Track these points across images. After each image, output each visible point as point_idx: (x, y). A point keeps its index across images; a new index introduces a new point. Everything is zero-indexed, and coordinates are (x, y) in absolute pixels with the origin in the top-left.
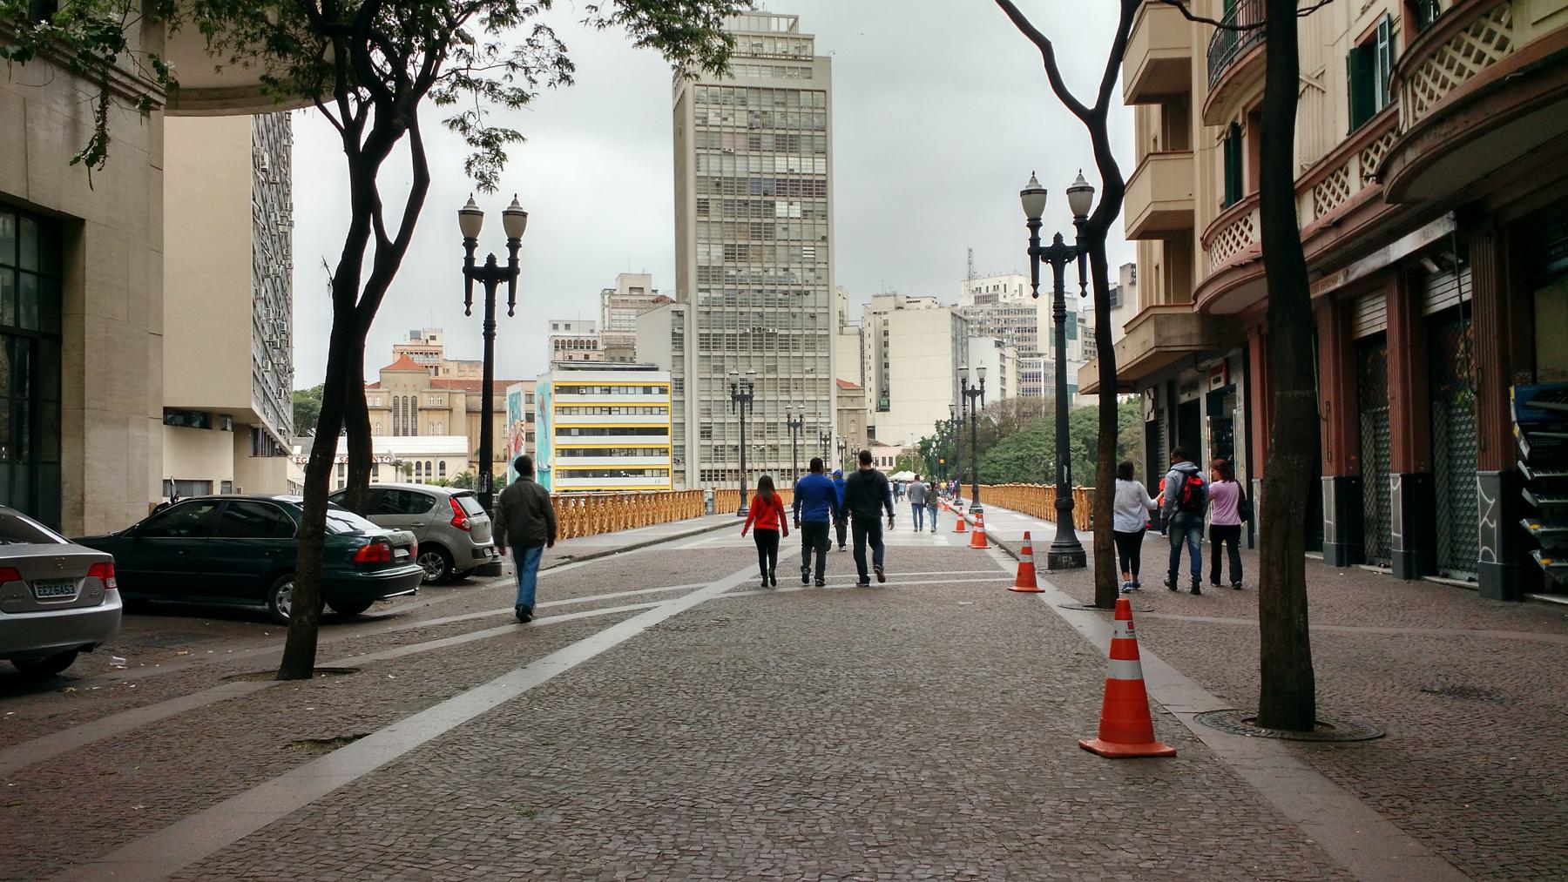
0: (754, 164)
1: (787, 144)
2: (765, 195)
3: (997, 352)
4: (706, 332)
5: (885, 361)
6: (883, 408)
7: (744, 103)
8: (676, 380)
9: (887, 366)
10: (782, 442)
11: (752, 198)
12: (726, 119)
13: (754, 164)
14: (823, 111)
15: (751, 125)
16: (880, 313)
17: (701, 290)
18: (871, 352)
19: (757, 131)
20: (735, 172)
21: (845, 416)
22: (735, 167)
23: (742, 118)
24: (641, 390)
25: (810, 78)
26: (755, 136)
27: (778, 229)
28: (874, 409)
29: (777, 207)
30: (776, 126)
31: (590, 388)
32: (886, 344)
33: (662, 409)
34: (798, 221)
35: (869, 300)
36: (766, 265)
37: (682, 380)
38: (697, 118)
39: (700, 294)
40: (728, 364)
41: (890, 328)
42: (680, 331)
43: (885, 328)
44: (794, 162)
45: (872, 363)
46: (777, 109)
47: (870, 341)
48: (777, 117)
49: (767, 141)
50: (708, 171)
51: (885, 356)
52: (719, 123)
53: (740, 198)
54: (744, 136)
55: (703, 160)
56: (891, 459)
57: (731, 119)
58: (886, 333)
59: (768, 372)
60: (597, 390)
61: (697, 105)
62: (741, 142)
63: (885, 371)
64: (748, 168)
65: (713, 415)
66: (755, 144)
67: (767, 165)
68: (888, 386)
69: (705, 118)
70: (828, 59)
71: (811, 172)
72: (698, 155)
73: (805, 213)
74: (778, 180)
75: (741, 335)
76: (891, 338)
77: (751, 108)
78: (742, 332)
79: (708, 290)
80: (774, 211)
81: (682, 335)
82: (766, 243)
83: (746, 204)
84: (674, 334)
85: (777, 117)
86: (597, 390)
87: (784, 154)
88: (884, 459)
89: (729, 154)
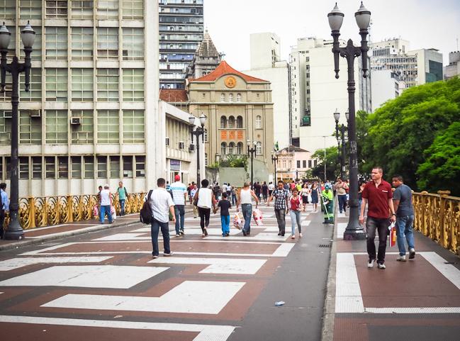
3: (394, 80)
5: (307, 88)
6: (306, 122)
9: (308, 92)
10: (49, 106)
16: (303, 52)
18: (296, 81)
21: (250, 111)
28: (299, 124)
32: (308, 76)
35: (295, 43)
41: (310, 63)
43: (307, 64)
45: (297, 89)
47: (296, 72)
51: (308, 84)
56: (304, 162)
58: (308, 67)
63: (307, 96)
68: (309, 106)
76: (311, 72)
88: (304, 162)
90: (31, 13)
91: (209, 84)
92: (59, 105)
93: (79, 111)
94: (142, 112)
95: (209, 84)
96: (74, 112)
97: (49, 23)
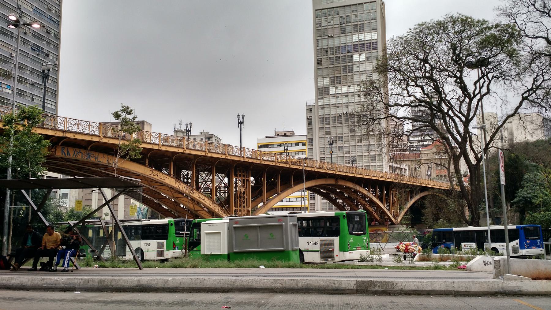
0: (343, 40)
1: (359, 28)
2: (348, 52)
4: (322, 117)
7: (338, 14)
8: (310, 139)
11: (342, 55)
12: (329, 22)
13: (343, 40)
14: (375, 11)
15: (341, 22)
17: (319, 99)
19: (344, 25)
20: (334, 45)
22: (334, 42)
23: (337, 21)
24: (294, 145)
26: (343, 27)
27: (355, 67)
29: (354, 57)
30: (352, 21)
31: (272, 145)
33: (303, 152)
34: (364, 62)
36: (349, 84)
37: (312, 139)
38: (317, 24)
39: (319, 100)
40: (332, 130)
42: (310, 118)
44: (362, 36)
46: (353, 14)
48: (353, 17)
49: (348, 29)
50: (322, 46)
52: (327, 25)
53: (337, 56)
54: (338, 28)
55: (320, 42)
57: (332, 22)
59: (351, 132)
60: (276, 146)
61: (317, 19)
62: (337, 31)
64: (340, 42)
65: (326, 154)
66: (343, 31)
67: (348, 39)
69: (321, 23)
71: (370, 39)
72: (317, 40)
73: (368, 58)
74: (354, 45)
75: (338, 117)
77: (340, 16)
78: (338, 115)
79: (322, 98)
80: (352, 59)
81: (311, 119)
82: (349, 74)
83: (339, 58)
84: (308, 119)
85: (353, 17)
86: (276, 146)
87: (356, 33)
89: (332, 37)
90: (353, 142)
91: (429, 150)
92: (361, 165)
93: (366, 166)
94: (382, 165)
95: (429, 150)
96: (365, 166)
97: (358, 144)
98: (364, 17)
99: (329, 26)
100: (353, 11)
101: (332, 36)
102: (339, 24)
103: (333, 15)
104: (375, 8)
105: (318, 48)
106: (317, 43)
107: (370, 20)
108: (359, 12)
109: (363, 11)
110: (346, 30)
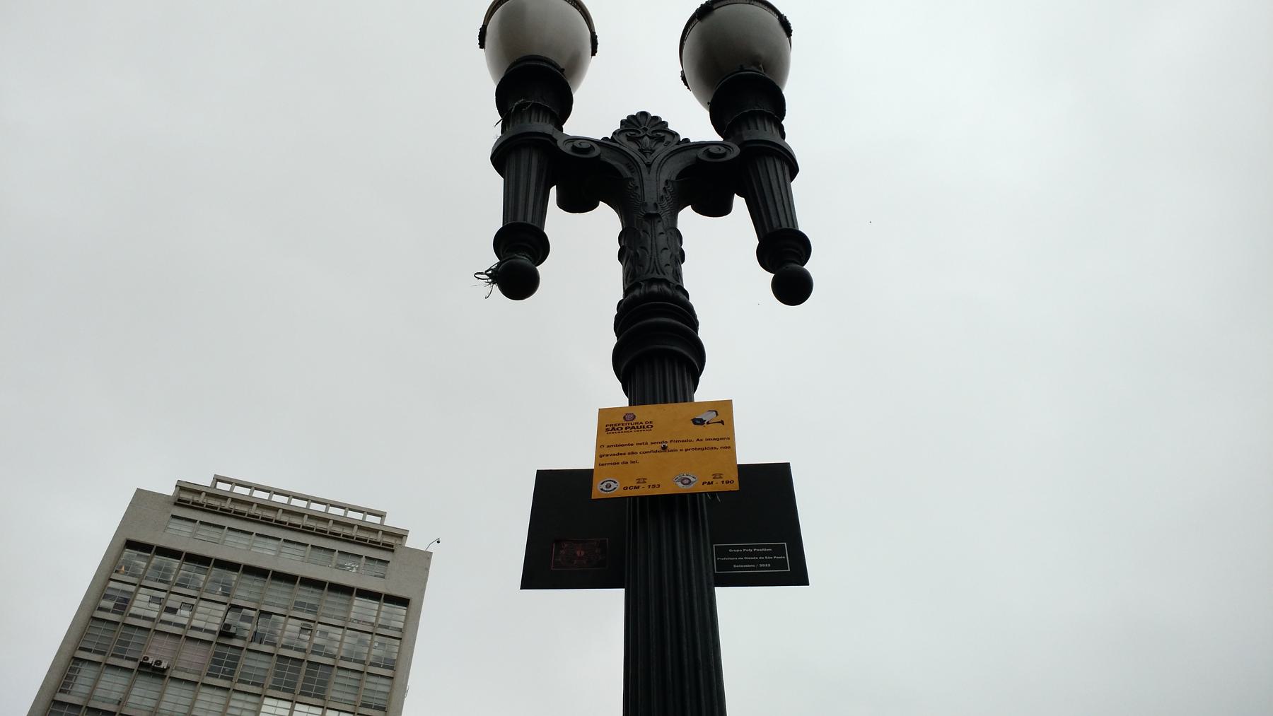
12: (173, 611)
14: (397, 634)
22: (159, 700)
23: (210, 617)
25: (383, 577)
49: (253, 664)
52: (154, 615)
54: (203, 647)
55: (87, 674)
62: (193, 659)
69: (126, 601)
70: (427, 556)
72: (77, 660)
77: (234, 602)
98: (341, 641)
99: (163, 622)
100: (296, 603)
101: (164, 665)
102: (213, 632)
103: (198, 589)
104: (401, 625)
105: (61, 697)
106: (68, 677)
107: (363, 662)
108: (323, 615)
109: (344, 619)
110: (239, 668)
